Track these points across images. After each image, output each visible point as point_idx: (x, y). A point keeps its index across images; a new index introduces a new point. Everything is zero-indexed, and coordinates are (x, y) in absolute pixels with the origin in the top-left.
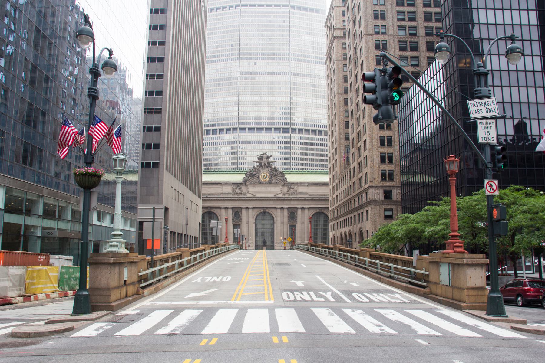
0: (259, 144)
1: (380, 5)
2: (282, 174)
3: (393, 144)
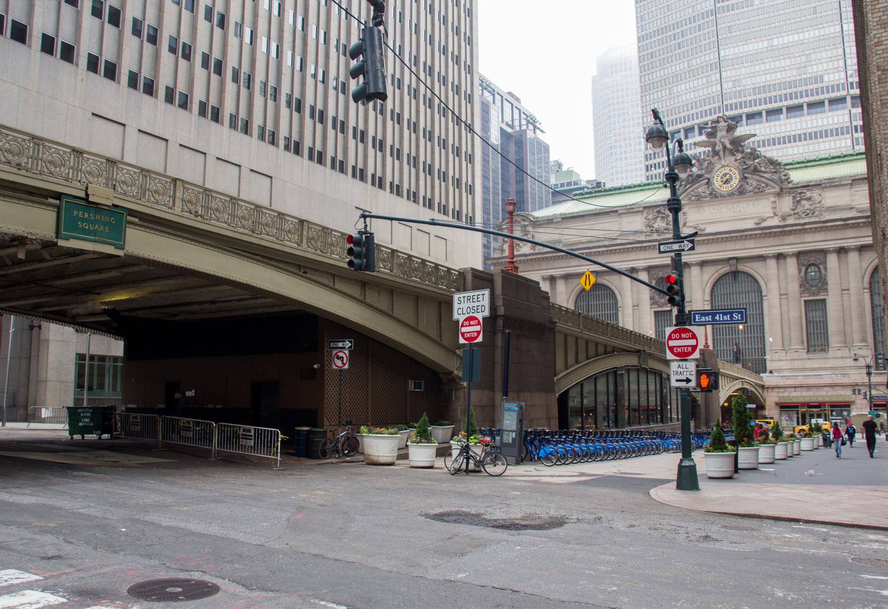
0: (774, 144)
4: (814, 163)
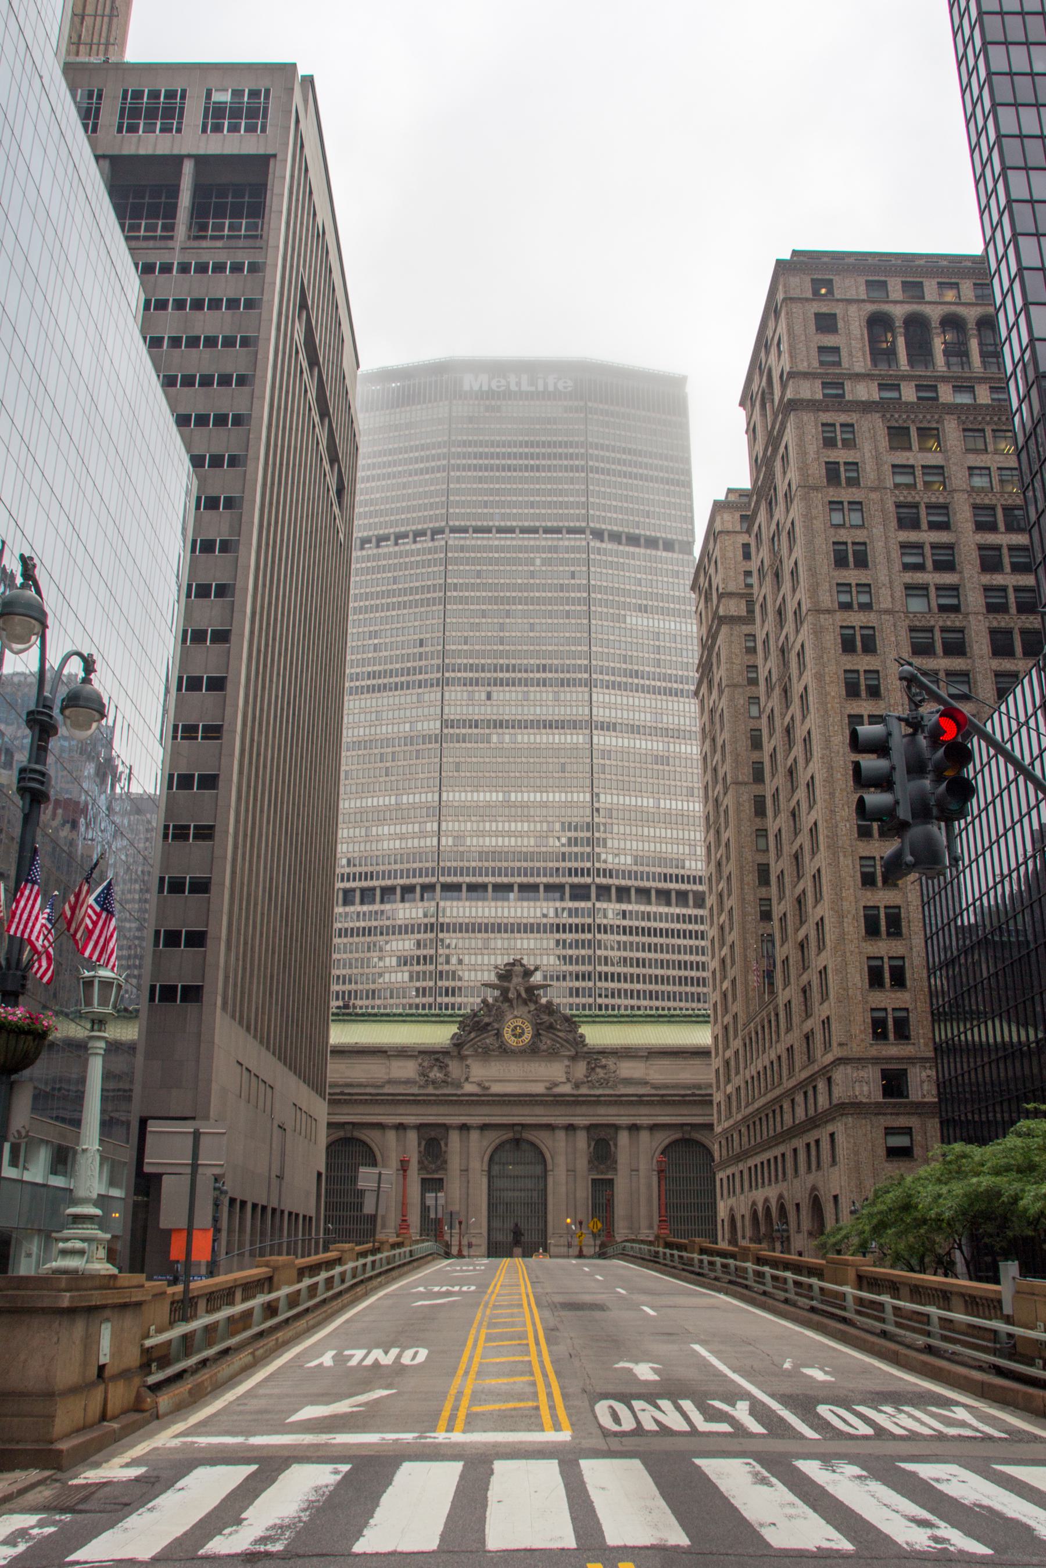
1: (852, 526)
2: (571, 1023)
3: (904, 930)
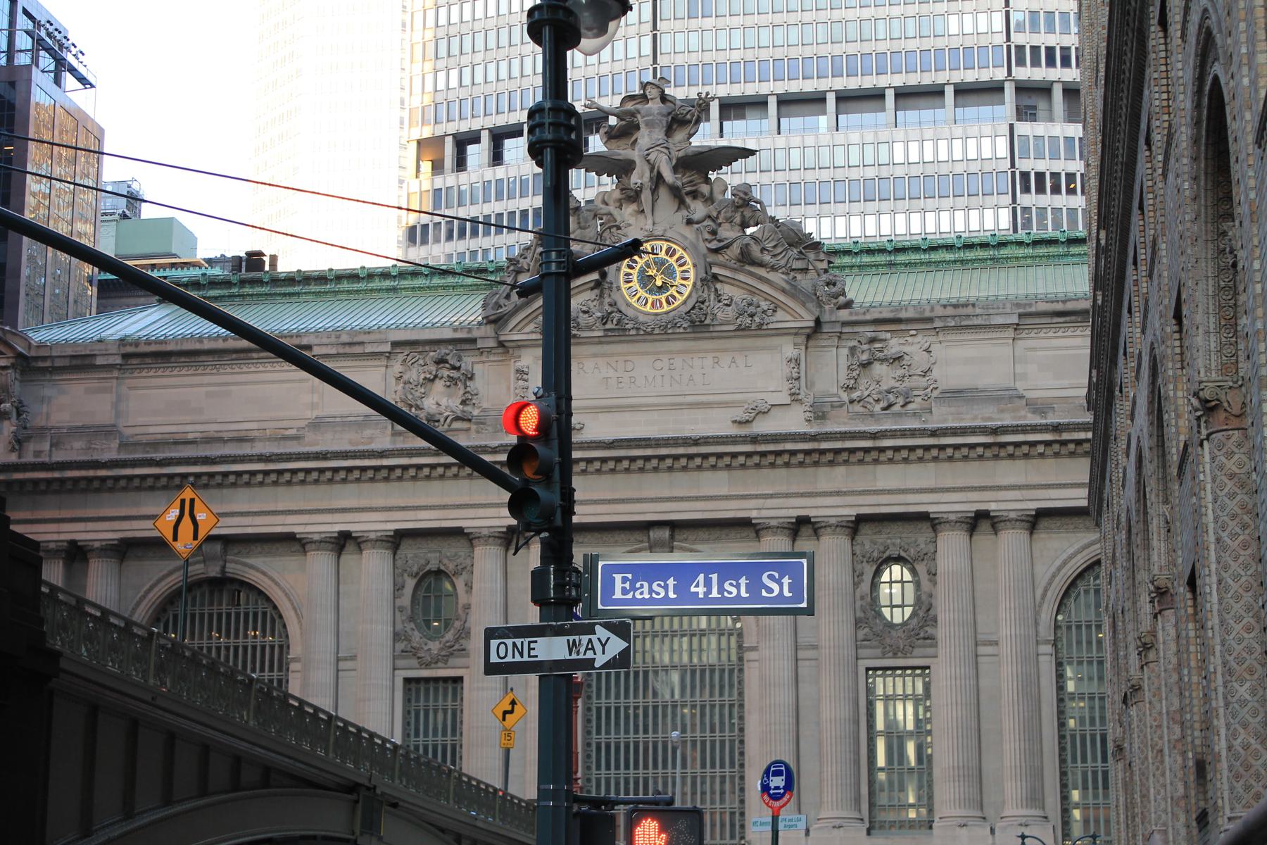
4: (914, 257)
